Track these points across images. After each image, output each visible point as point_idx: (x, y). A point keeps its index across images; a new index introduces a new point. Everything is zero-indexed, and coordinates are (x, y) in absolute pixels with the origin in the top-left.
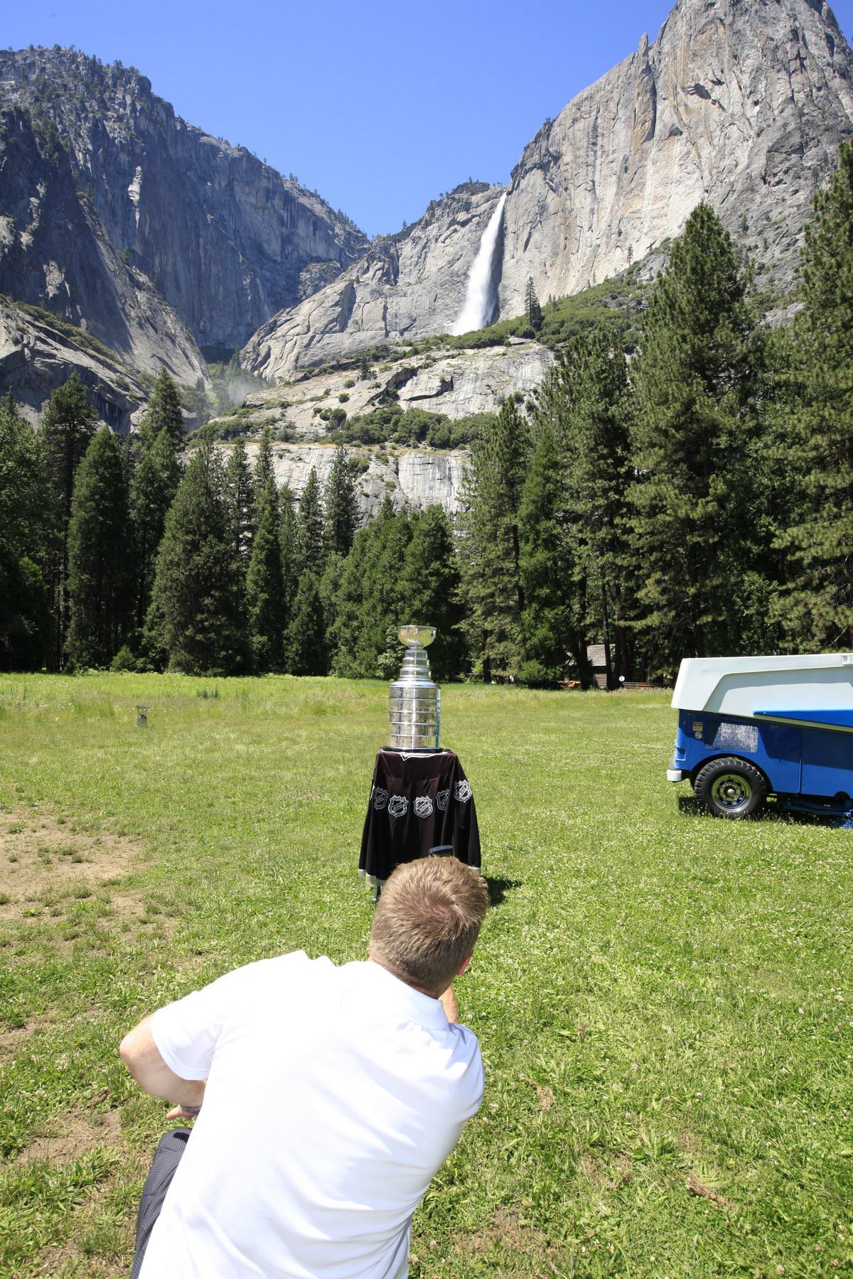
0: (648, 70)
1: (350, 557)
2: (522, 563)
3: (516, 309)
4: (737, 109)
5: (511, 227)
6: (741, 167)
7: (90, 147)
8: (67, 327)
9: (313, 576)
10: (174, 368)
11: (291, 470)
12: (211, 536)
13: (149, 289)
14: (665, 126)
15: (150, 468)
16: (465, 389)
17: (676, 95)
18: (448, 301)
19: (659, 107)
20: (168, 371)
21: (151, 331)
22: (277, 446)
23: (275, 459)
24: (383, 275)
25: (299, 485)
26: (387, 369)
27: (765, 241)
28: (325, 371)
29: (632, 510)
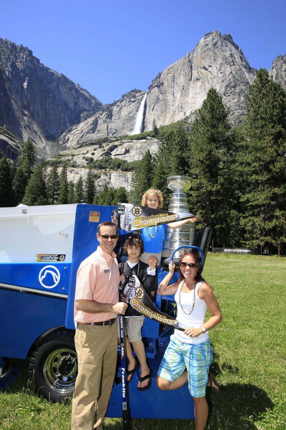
0: (190, 61)
3: (150, 128)
4: (216, 74)
5: (148, 104)
7: (11, 70)
11: (74, 177)
12: (41, 196)
13: (28, 116)
14: (195, 77)
16: (133, 152)
17: (198, 69)
18: (128, 125)
19: (193, 72)
20: (31, 141)
22: (69, 169)
23: (68, 173)
24: (107, 116)
25: (75, 182)
26: (107, 145)
28: (87, 145)
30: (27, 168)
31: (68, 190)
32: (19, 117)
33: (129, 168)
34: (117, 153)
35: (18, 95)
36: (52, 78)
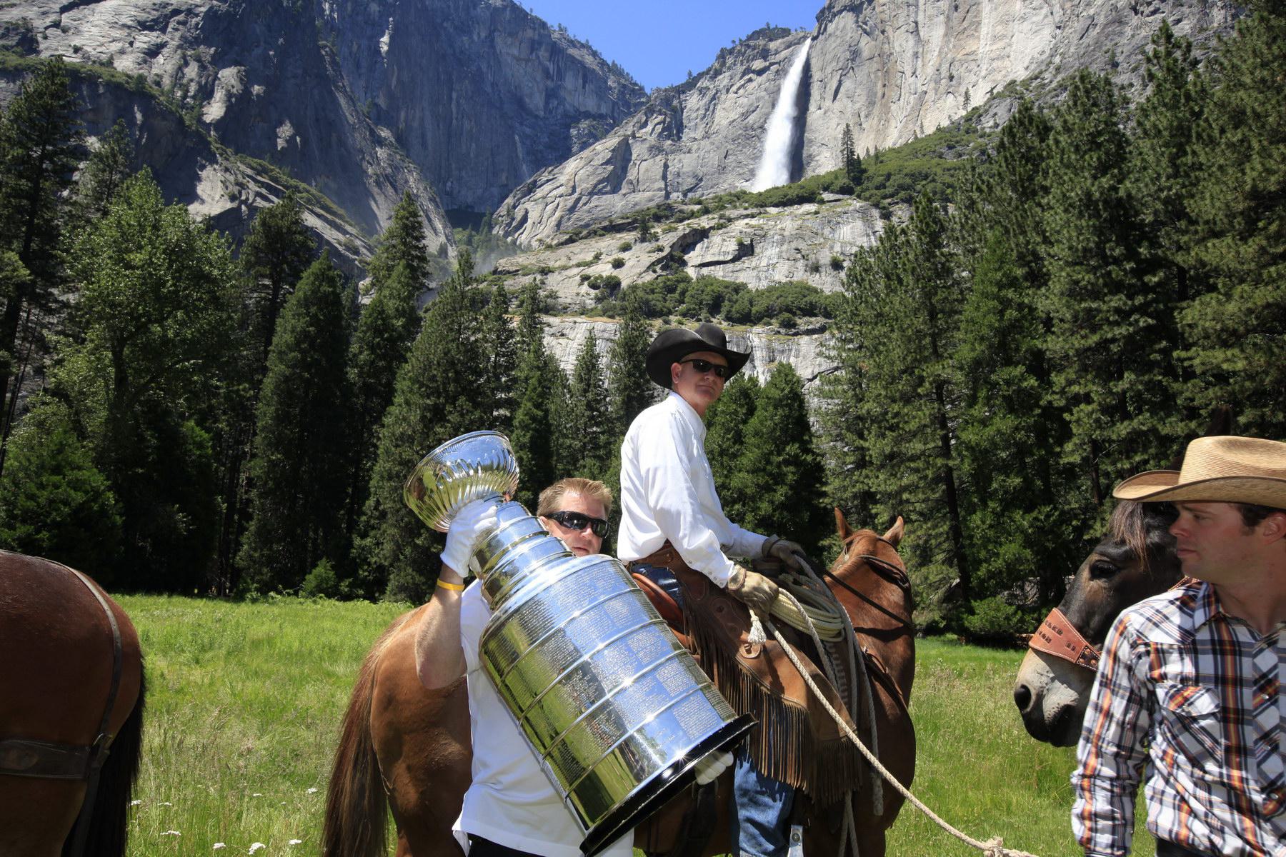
3: (826, 162)
5: (816, 75)
13: (391, 145)
16: (768, 253)
18: (741, 157)
21: (390, 190)
24: (663, 130)
26: (671, 230)
28: (595, 232)
32: (361, 151)
33: (754, 312)
34: (708, 259)
35: (360, 75)
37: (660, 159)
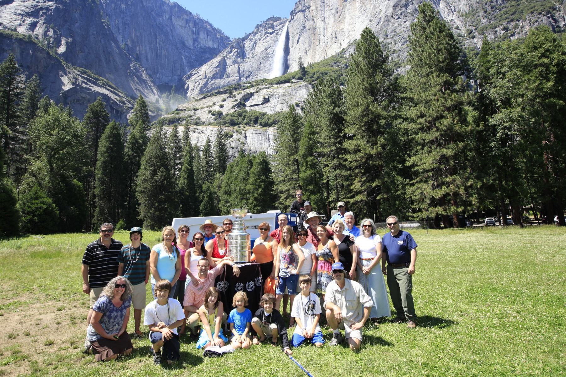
1: (225, 175)
2: (301, 175)
5: (291, 35)
6: (383, 12)
8: (97, 77)
9: (209, 184)
10: (146, 95)
11: (198, 137)
15: (134, 138)
16: (274, 101)
18: (265, 65)
20: (143, 96)
21: (135, 79)
22: (192, 127)
23: (191, 133)
24: (237, 54)
25: (202, 144)
26: (240, 93)
27: (395, 41)
29: (346, 151)
30: (140, 133)
31: (193, 157)
34: (253, 104)
36: (163, 8)
37: (237, 65)
